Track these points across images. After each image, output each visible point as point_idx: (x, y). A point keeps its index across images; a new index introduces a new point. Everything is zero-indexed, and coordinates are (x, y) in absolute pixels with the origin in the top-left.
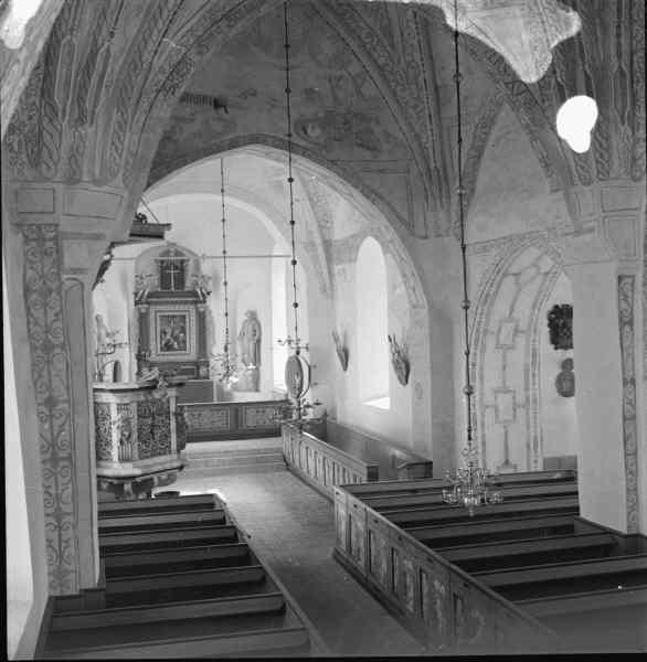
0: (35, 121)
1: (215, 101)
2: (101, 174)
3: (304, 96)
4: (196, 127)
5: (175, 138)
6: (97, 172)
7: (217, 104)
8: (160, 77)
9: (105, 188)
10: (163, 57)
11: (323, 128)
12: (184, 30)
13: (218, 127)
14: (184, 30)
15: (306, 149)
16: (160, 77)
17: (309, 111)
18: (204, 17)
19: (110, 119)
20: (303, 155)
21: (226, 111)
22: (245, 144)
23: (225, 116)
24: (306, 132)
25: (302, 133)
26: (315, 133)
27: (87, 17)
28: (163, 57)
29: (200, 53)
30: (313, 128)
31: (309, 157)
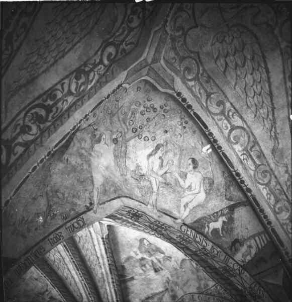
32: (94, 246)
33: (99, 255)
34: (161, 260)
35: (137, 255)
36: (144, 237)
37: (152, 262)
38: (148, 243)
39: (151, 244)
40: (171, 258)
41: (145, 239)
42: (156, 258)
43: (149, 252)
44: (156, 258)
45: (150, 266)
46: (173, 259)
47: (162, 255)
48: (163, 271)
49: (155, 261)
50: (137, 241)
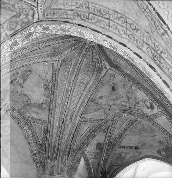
0: (44, 160)
1: (136, 147)
2: (60, 171)
3: (159, 143)
4: (131, 155)
5: (126, 158)
6: (59, 171)
7: (136, 148)
8: (78, 147)
9: (61, 175)
10: (78, 143)
11: (166, 152)
12: (83, 136)
13: (136, 154)
14: (83, 136)
15: (161, 158)
16: (78, 147)
17: (161, 147)
18: (88, 132)
19: (63, 158)
20: (161, 160)
21: (139, 150)
22: (144, 158)
23: (138, 151)
24: (161, 154)
25: (160, 154)
26: (163, 153)
27: (54, 136)
28: (79, 141)
29: (87, 140)
30: (163, 152)
31: (163, 161)
32: (37, 54)
33: (30, 56)
34: (19, 83)
35: (21, 71)
36: (32, 72)
37: (16, 79)
38: (28, 74)
39: (28, 75)
40: (22, 87)
41: (31, 72)
42: (19, 80)
43: (22, 75)
44: (19, 80)
45: (14, 78)
46: (22, 89)
47: (22, 83)
48: (13, 86)
49: (17, 80)
50: (30, 68)
